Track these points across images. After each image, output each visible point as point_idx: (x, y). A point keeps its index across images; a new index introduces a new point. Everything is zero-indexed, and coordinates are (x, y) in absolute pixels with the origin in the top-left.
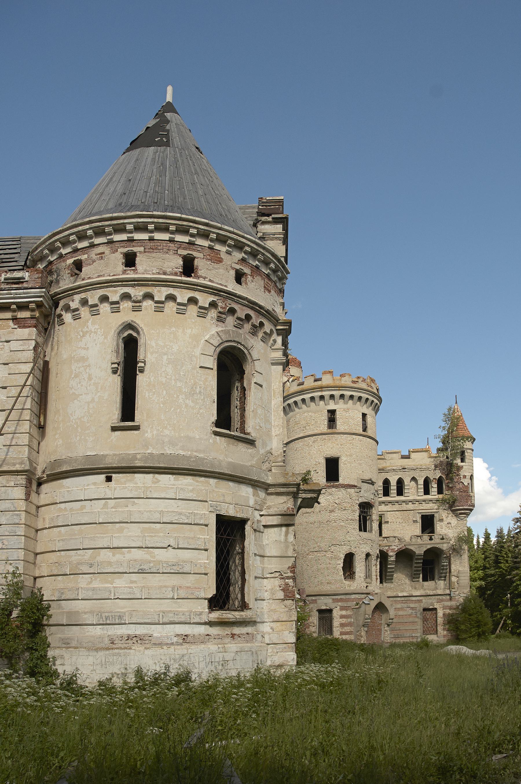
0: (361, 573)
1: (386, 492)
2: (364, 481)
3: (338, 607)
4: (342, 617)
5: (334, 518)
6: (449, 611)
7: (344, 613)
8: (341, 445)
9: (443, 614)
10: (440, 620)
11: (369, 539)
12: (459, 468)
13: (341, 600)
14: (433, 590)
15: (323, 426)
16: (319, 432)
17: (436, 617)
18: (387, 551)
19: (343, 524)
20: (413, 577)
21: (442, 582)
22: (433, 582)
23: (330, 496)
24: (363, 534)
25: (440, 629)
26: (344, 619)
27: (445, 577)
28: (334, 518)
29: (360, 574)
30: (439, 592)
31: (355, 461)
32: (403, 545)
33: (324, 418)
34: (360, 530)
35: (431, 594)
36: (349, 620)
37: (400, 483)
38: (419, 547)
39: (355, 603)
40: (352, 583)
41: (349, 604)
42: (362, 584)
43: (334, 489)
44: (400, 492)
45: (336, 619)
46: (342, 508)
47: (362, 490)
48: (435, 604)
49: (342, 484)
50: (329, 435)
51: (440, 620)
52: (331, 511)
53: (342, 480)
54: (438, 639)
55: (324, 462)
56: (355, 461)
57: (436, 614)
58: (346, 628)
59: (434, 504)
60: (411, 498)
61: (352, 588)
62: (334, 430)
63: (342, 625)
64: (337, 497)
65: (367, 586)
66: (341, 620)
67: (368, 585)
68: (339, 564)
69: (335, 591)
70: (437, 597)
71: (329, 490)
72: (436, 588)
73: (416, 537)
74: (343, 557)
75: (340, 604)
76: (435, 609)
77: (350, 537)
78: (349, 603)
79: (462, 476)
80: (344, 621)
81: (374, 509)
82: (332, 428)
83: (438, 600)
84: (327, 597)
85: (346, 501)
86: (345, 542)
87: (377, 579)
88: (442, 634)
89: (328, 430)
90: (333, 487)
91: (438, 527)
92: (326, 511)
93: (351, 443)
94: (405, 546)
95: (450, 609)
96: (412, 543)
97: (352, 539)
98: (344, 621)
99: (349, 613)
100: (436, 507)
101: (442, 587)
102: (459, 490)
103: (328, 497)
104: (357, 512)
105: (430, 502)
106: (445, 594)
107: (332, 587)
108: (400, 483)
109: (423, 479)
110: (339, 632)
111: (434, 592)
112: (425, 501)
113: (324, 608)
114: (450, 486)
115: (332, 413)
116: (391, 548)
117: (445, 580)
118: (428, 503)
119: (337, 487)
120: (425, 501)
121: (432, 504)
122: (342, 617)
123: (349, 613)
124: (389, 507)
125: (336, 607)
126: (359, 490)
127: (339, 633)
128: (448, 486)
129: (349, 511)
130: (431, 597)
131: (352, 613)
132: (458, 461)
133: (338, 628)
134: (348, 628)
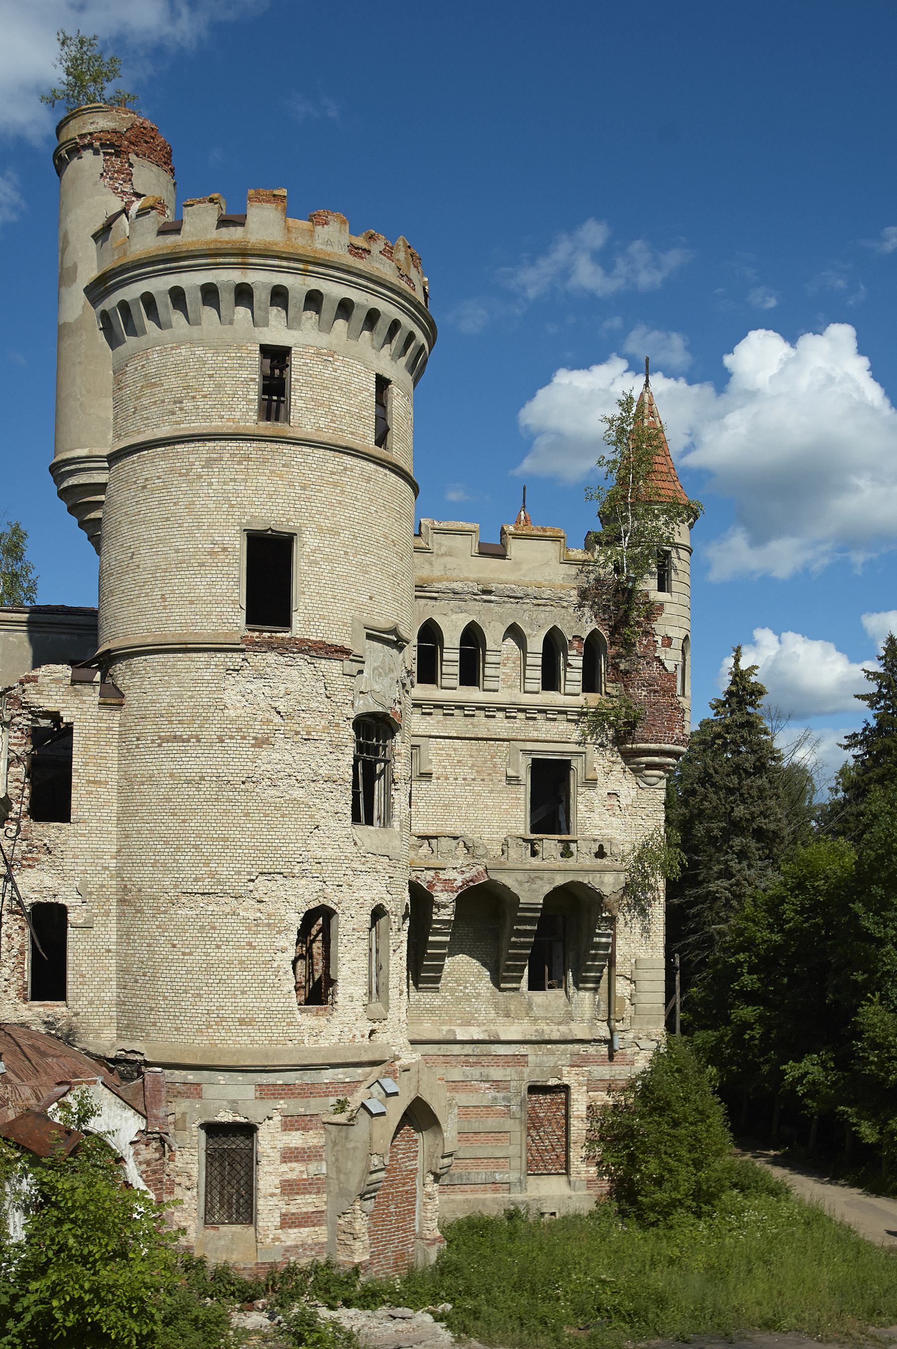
0: (355, 984)
3: (277, 1118)
4: (290, 1155)
5: (269, 767)
6: (607, 1098)
8: (304, 488)
9: (588, 1108)
10: (579, 1128)
11: (384, 852)
12: (653, 611)
13: (286, 1091)
14: (560, 1024)
16: (227, 426)
17: (567, 1117)
18: (431, 885)
19: (298, 793)
21: (586, 997)
22: (560, 992)
23: (260, 683)
24: (362, 831)
25: (577, 1154)
26: (294, 1165)
27: (597, 980)
28: (269, 767)
29: (351, 989)
30: (579, 1030)
31: (346, 553)
32: (481, 869)
35: (555, 1036)
36: (313, 1168)
38: (531, 881)
39: (333, 1100)
40: (323, 1021)
41: (315, 1105)
42: (358, 1024)
43: (271, 657)
45: (271, 1162)
46: (297, 733)
47: (366, 668)
48: (565, 1070)
49: (303, 641)
50: (263, 445)
52: (261, 742)
54: (573, 1193)
55: (240, 545)
56: (346, 553)
57: (567, 1104)
58: (300, 1199)
59: (572, 726)
61: (324, 1043)
62: (278, 428)
63: (290, 1188)
64: (282, 688)
65: (372, 1032)
66: (285, 1167)
67: (376, 1026)
68: (283, 950)
69: (266, 1055)
70: (570, 1047)
71: (257, 660)
72: (569, 1018)
73: (521, 842)
75: (282, 1104)
76: (566, 1088)
77: (323, 847)
78: (313, 1101)
79: (659, 639)
80: (295, 1171)
81: (398, 737)
82: (277, 420)
83: (575, 1058)
84: (240, 1077)
85: (314, 705)
86: (306, 866)
88: (583, 1175)
89: (262, 424)
91: (580, 807)
92: (244, 738)
93: (335, 485)
94: (486, 870)
95: (609, 1091)
96: (509, 865)
97: (329, 852)
98: (295, 1171)
99: (313, 1139)
100: (576, 736)
101: (587, 1016)
102: (648, 684)
103: (252, 687)
104: (347, 751)
105: (559, 717)
106: (595, 1041)
107: (258, 1036)
109: (543, 633)
110: (277, 1214)
111: (563, 1028)
112: (545, 712)
113: (225, 1117)
114: (622, 667)
116: (443, 875)
117: (595, 990)
118: (555, 720)
119: (282, 648)
120: (545, 712)
121: (566, 724)
122: (290, 1155)
123: (313, 1139)
125: (270, 1118)
126: (357, 666)
127: (277, 1221)
128: (615, 667)
129: (322, 747)
130: (554, 1046)
131: (322, 1141)
132: (649, 584)
133: (274, 1201)
134: (310, 1198)
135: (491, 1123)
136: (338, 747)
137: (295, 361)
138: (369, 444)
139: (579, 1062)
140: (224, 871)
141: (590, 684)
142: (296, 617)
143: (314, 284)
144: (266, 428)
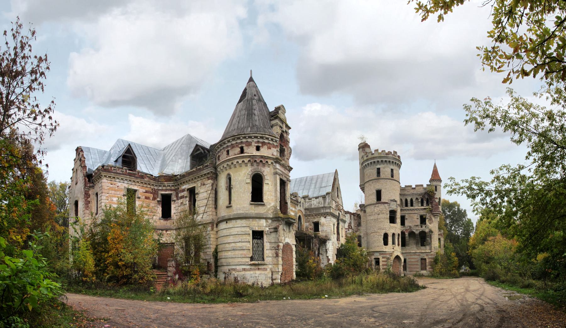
1: (406, 205)
2: (391, 201)
15: (375, 176)
20: (417, 244)
24: (392, 225)
25: (427, 268)
33: (375, 172)
34: (390, 222)
37: (412, 200)
44: (412, 205)
51: (427, 264)
52: (379, 214)
53: (382, 201)
55: (375, 192)
60: (416, 208)
71: (377, 205)
87: (398, 245)
90: (379, 203)
108: (412, 200)
124: (407, 212)
135: (416, 263)
136: (387, 214)
138: (390, 177)
139: (427, 255)
140: (375, 229)
141: (428, 204)
144: (378, 178)
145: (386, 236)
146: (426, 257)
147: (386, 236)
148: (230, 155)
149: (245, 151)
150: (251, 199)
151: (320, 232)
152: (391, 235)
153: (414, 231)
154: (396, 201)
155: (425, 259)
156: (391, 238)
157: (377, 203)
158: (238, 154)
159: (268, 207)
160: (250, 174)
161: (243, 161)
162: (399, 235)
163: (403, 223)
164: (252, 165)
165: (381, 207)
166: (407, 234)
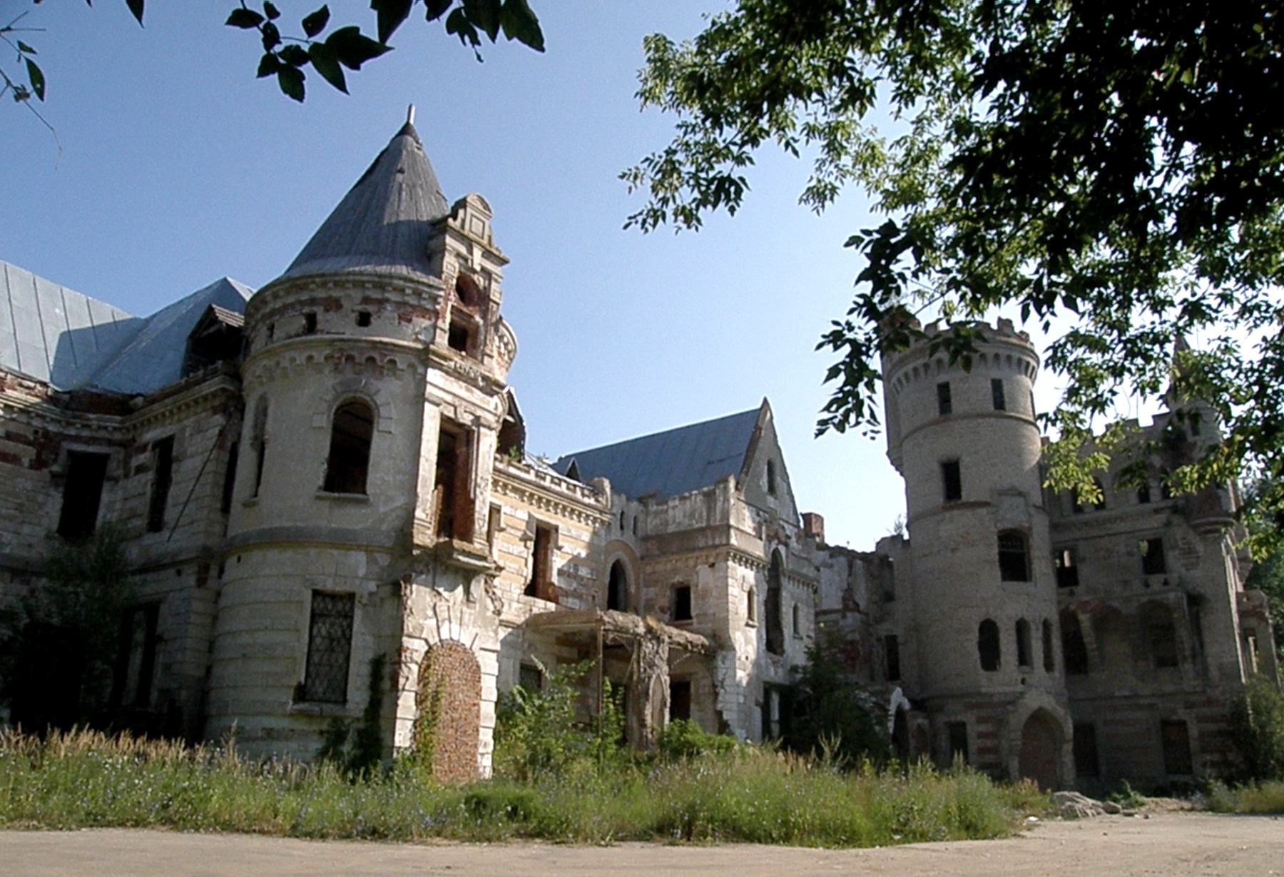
2: (1002, 493)
7: (983, 728)
24: (1013, 586)
33: (932, 399)
43: (955, 512)
57: (1186, 730)
74: (976, 628)
87: (1049, 666)
90: (952, 508)
115: (944, 389)
119: (959, 507)
137: (952, 387)
142: (963, 494)
143: (996, 351)
145: (989, 632)
146: (1182, 714)
147: (989, 632)
148: (275, 337)
149: (319, 327)
150: (321, 482)
151: (695, 620)
152: (1012, 625)
153: (1115, 604)
154: (1020, 494)
155: (1182, 724)
156: (1014, 638)
157: (945, 509)
158: (298, 335)
159: (382, 510)
160: (329, 397)
161: (310, 358)
162: (1046, 625)
163: (1066, 578)
164: (336, 369)
165: (961, 521)
166: (1085, 619)
